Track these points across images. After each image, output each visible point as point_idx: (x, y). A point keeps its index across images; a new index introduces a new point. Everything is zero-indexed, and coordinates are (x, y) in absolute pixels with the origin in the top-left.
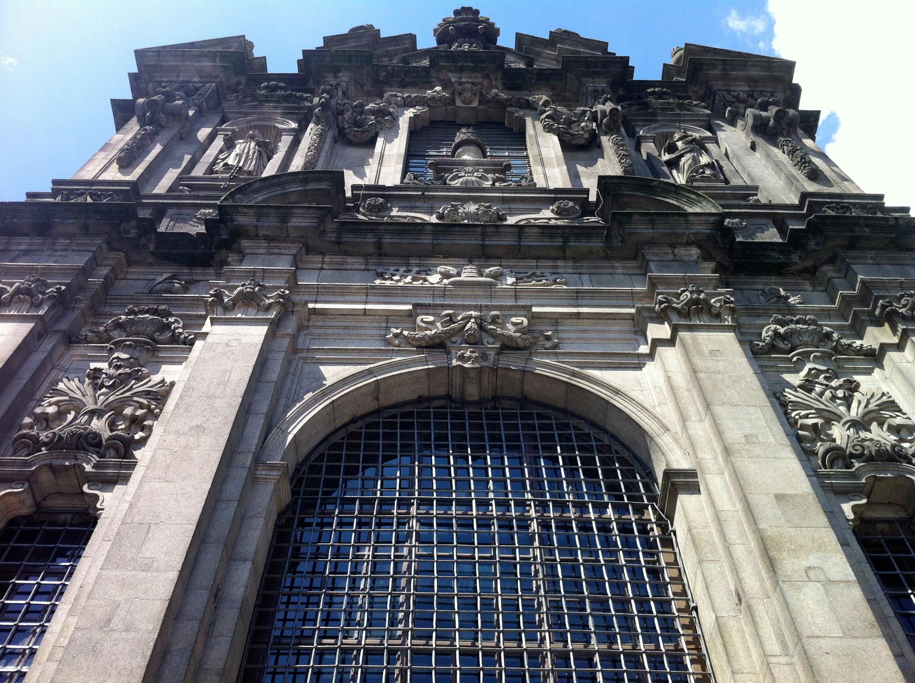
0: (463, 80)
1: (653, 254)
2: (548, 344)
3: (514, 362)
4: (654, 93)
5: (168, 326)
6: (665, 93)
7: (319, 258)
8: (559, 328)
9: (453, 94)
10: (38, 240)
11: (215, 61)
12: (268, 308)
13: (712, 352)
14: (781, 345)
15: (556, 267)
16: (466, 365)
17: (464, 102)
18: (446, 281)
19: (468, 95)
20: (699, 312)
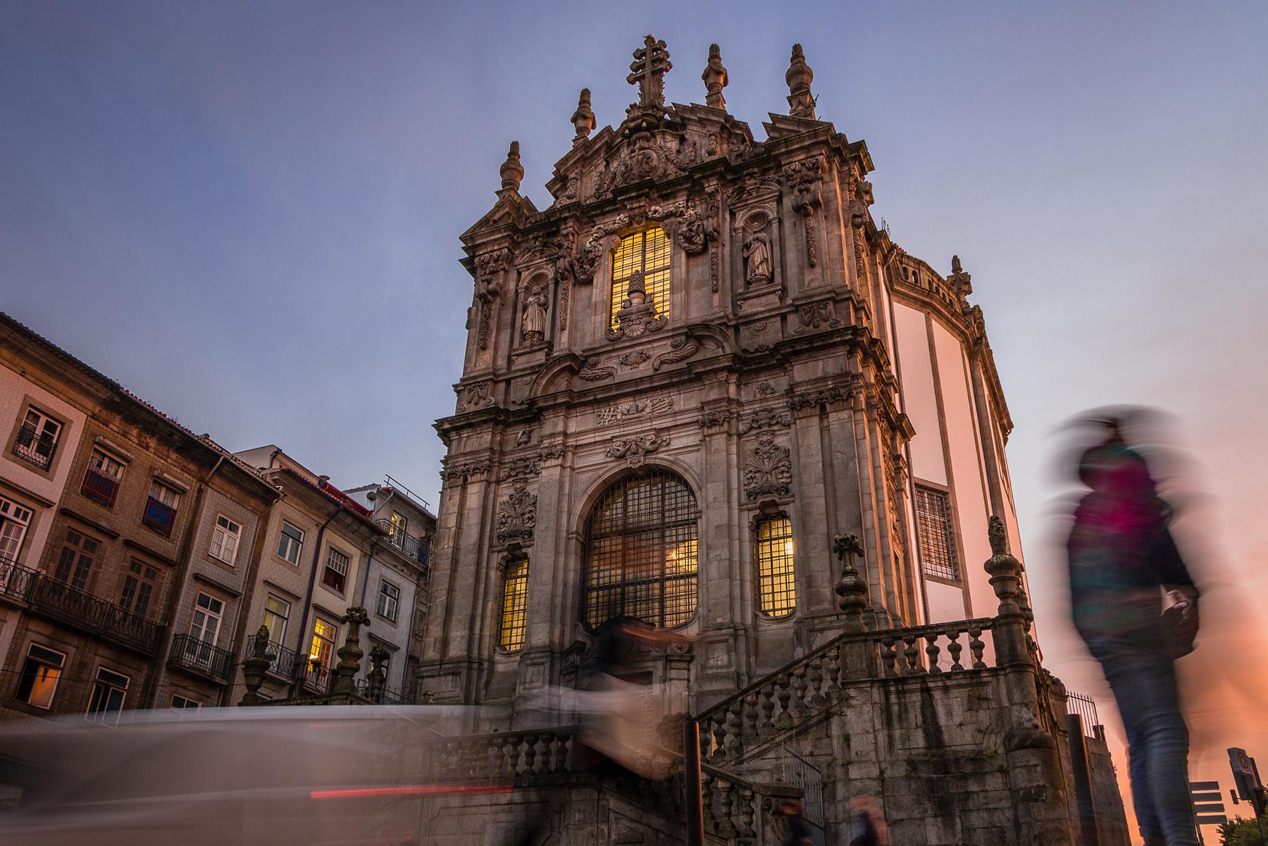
0: (634, 206)
1: (708, 380)
2: (665, 444)
3: (651, 460)
4: (747, 175)
9: (629, 217)
11: (501, 232)
12: (558, 458)
19: (637, 219)
20: (716, 424)
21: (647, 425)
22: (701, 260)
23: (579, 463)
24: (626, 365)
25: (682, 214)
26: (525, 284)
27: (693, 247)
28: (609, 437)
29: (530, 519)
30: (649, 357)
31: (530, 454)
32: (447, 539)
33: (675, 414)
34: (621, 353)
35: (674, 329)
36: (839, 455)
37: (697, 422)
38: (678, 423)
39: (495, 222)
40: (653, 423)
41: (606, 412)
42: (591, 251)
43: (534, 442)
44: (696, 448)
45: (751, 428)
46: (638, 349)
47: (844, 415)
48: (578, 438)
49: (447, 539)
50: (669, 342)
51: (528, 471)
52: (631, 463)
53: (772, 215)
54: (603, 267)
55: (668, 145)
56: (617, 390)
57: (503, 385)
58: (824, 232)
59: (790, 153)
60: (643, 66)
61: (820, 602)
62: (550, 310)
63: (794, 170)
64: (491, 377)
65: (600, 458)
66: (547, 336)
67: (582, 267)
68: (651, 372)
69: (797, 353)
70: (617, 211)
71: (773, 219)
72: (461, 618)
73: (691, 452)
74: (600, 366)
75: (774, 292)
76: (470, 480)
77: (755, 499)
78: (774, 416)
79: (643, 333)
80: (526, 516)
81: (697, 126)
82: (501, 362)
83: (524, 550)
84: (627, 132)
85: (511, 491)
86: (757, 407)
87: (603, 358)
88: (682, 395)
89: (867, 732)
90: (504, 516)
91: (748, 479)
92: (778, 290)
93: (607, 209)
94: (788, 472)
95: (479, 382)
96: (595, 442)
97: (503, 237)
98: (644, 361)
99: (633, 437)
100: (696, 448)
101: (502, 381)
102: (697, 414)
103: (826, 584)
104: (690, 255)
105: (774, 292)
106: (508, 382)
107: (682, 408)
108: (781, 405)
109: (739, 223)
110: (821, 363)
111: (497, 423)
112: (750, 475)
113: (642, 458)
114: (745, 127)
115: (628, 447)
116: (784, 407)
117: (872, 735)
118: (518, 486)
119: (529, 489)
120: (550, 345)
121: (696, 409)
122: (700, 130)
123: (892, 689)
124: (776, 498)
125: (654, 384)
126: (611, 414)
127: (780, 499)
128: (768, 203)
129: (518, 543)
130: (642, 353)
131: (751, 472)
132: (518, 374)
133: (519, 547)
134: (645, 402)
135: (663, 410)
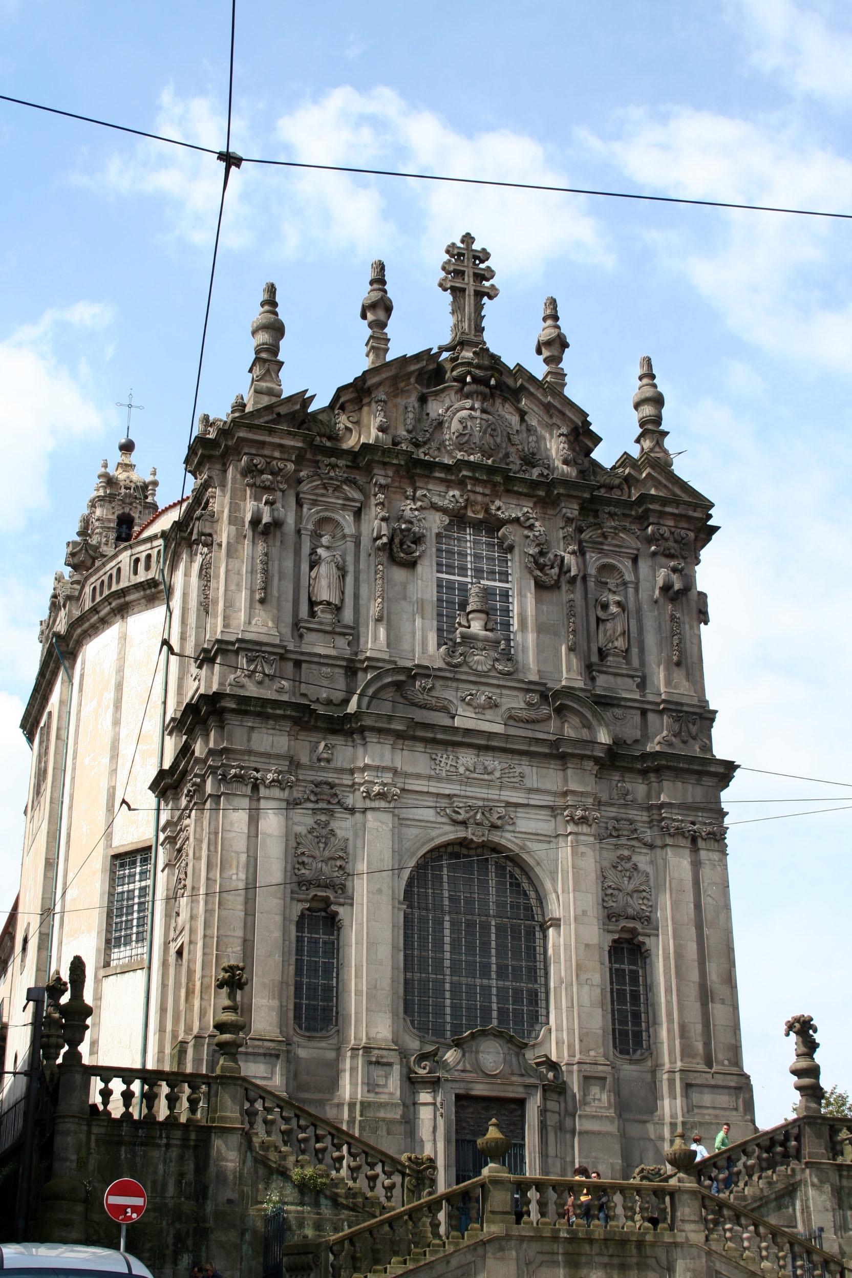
5: (336, 795)
6: (616, 514)
7: (401, 742)
8: (518, 810)
9: (467, 500)
10: (258, 720)
13: (582, 853)
14: (614, 834)
15: (521, 760)
16: (475, 839)
17: (473, 512)
18: (468, 773)
19: (478, 507)
20: (582, 823)
21: (493, 794)
22: (546, 595)
23: (404, 813)
24: (469, 704)
25: (531, 527)
26: (310, 527)
27: (544, 578)
28: (447, 792)
29: (341, 866)
30: (496, 706)
31: (331, 777)
32: (234, 866)
33: (531, 790)
34: (461, 686)
35: (530, 682)
36: (709, 900)
37: (552, 808)
38: (532, 802)
39: (278, 414)
40: (503, 793)
41: (446, 760)
42: (411, 523)
43: (338, 763)
44: (548, 839)
45: (611, 836)
46: (482, 688)
47: (715, 856)
48: (407, 781)
49: (234, 866)
50: (520, 695)
51: (335, 801)
52: (473, 834)
53: (629, 577)
54: (428, 552)
55: (508, 416)
56: (463, 737)
57: (290, 665)
58: (687, 627)
59: (662, 514)
60: (459, 273)
61: (693, 1056)
62: (350, 579)
63: (662, 535)
64: (282, 651)
65: (429, 814)
66: (348, 615)
67: (402, 543)
68: (499, 728)
69: (668, 768)
70: (449, 484)
71: (631, 582)
72: (267, 982)
73: (541, 841)
74: (434, 693)
75: (632, 677)
76: (263, 792)
77: (617, 921)
78: (636, 830)
79: (490, 670)
80: (338, 863)
81: (538, 407)
82: (287, 630)
83: (334, 908)
84: (468, 379)
85: (310, 821)
86: (612, 812)
87: (439, 683)
88: (535, 769)
89: (827, 1210)
90: (303, 854)
91: (606, 895)
92: (638, 677)
93: (437, 474)
94: (648, 900)
95: (264, 652)
96: (428, 792)
97: (293, 447)
98: (491, 708)
99: (480, 803)
100: (548, 839)
101: (291, 659)
102: (552, 799)
103: (699, 1038)
104: (540, 586)
105: (632, 677)
106: (298, 664)
107: (535, 786)
108: (639, 818)
109: (592, 571)
110: (690, 787)
111: (296, 721)
112: (610, 891)
113: (487, 832)
114: (597, 440)
115: (472, 813)
116: (644, 822)
117: (831, 1214)
118: (323, 818)
119: (334, 825)
120: (353, 633)
121: (555, 794)
122: (541, 413)
123: (845, 1173)
124: (639, 926)
125: (508, 746)
126: (449, 762)
127: (643, 928)
128: (623, 557)
129: (328, 897)
130: (490, 698)
131: (610, 887)
132: (316, 660)
133: (327, 901)
134: (493, 763)
135: (513, 780)
